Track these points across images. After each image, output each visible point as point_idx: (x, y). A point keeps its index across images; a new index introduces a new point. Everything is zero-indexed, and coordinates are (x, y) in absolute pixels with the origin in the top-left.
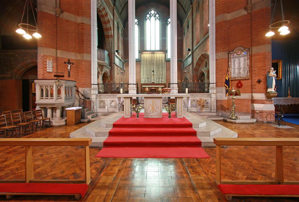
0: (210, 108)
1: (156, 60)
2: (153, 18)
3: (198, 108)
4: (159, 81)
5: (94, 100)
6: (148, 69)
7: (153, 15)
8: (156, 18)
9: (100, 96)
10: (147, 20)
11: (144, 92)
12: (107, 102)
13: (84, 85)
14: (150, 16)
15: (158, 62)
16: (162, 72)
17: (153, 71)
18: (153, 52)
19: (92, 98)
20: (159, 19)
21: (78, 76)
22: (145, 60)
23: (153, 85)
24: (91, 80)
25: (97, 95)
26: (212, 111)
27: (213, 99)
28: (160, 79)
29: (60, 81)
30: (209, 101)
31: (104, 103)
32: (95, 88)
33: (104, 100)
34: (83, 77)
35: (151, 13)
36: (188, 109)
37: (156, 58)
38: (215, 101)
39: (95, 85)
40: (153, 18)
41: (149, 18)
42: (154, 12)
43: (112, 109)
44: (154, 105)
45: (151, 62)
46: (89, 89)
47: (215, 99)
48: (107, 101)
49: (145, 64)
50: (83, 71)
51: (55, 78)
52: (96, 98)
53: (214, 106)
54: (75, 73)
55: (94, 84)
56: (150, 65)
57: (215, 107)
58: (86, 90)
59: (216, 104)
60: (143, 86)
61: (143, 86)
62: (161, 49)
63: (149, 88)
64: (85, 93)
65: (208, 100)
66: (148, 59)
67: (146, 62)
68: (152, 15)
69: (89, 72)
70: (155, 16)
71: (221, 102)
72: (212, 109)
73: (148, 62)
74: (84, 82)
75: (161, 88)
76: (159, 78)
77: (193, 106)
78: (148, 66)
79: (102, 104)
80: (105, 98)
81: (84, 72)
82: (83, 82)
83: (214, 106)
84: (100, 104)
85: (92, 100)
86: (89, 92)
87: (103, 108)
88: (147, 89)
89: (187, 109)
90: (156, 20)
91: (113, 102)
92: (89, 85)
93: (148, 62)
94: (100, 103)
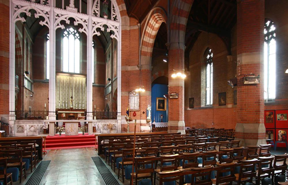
2: (71, 36)
4: (78, 107)
7: (72, 33)
8: (76, 37)
10: (64, 37)
14: (69, 34)
17: (72, 98)
18: (71, 74)
20: (80, 39)
22: (62, 81)
35: (69, 31)
40: (71, 36)
41: (67, 36)
42: (73, 30)
45: (69, 85)
49: (61, 87)
56: (68, 88)
60: (59, 112)
61: (59, 112)
62: (82, 73)
66: (65, 82)
68: (70, 33)
70: (74, 35)
73: (65, 85)
75: (80, 114)
78: (65, 89)
90: (76, 39)
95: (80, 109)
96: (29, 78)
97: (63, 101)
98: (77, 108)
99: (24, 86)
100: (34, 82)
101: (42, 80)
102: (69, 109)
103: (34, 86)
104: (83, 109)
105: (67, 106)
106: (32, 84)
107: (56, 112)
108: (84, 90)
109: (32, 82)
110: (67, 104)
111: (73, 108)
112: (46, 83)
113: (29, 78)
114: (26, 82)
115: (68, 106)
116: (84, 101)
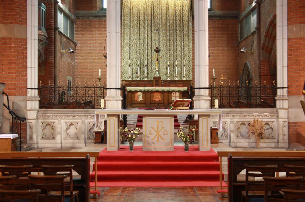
0: (276, 140)
1: (164, 13)
3: (251, 140)
4: (172, 75)
5: (34, 121)
6: (142, 38)
11: (132, 104)
13: (15, 89)
15: (171, 18)
16: (182, 50)
17: (158, 51)
21: (2, 70)
23: (157, 85)
25: (38, 111)
26: (280, 145)
27: (281, 121)
28: (177, 69)
30: (275, 125)
31: (53, 129)
33: (54, 123)
36: (230, 142)
37: (164, 9)
38: (286, 124)
43: (71, 141)
44: (160, 128)
47: (286, 120)
49: (134, 24)
52: (37, 118)
53: (284, 135)
56: (149, 28)
57: (286, 137)
59: (289, 131)
60: (129, 88)
61: (129, 88)
63: (144, 92)
65: (273, 122)
66: (141, 13)
67: (135, 19)
71: (295, 126)
72: (280, 141)
73: (142, 18)
74: (15, 84)
75: (178, 94)
76: (174, 66)
77: (242, 136)
79: (48, 130)
80: (56, 118)
82: (12, 84)
83: (284, 135)
84: (45, 131)
86: (22, 104)
87: (52, 139)
88: (140, 97)
89: (228, 141)
92: (23, 90)
93: (142, 18)
95: (177, 79)
96: (66, 10)
97: (138, 63)
98: (169, 79)
99: (56, 29)
100: (78, 17)
101: (93, 12)
102: (151, 81)
103: (78, 28)
104: (184, 79)
105: (146, 73)
106: (72, 23)
107: (123, 89)
108: (186, 28)
109: (73, 17)
110: (148, 69)
111: (159, 78)
112: (101, 17)
113: (66, 10)
114: (60, 18)
115: (148, 73)
116: (187, 58)
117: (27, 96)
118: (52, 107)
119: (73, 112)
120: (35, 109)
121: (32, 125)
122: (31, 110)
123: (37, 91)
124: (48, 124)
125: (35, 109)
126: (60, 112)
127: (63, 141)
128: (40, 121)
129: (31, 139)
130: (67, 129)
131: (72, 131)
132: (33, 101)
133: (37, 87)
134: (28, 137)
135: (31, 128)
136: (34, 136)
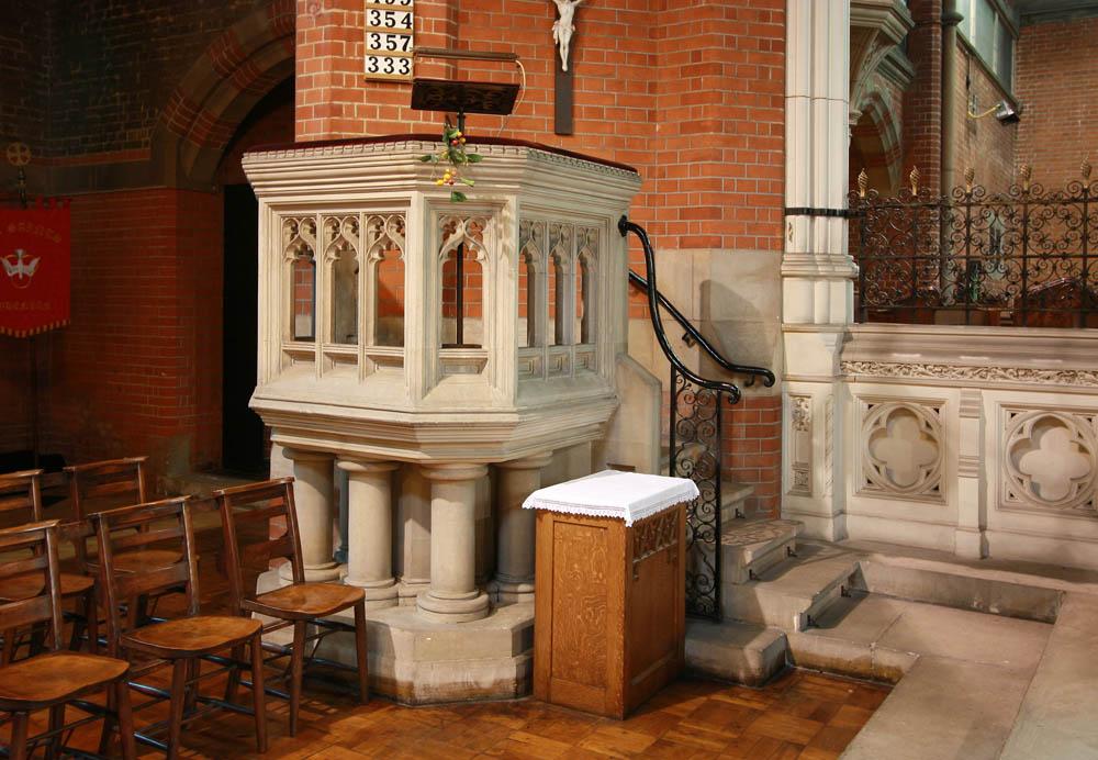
5: (819, 392)
9: (883, 349)
12: (969, 425)
13: (715, 213)
19: (790, 372)
21: (652, 116)
24: (783, 159)
25: (847, 338)
29: (470, 149)
31: (930, 438)
32: (828, 259)
34: (700, 127)
39: (820, 220)
43: (1048, 523)
46: (752, 260)
48: (972, 410)
50: (697, 56)
51: (433, 121)
52: (840, 375)
54: (619, 85)
55: (811, 212)
58: (732, 270)
64: (716, 314)
69: (764, 72)
74: (715, 184)
80: (947, 378)
81: (718, 69)
82: (698, 184)
84: (882, 445)
85: (796, 387)
86: (754, 295)
91: (1054, 433)
92: (762, 217)
94: (873, 437)
117: (783, 249)
118: (928, 319)
119: (1062, 350)
120: (827, 325)
121: (811, 408)
122: (808, 326)
123: (839, 227)
124: (903, 411)
125: (827, 325)
126: (975, 348)
127: (993, 517)
128: (856, 388)
129: (805, 486)
130: (1019, 448)
131: (1053, 458)
132: (815, 277)
133: (839, 204)
134: (789, 477)
135: (803, 425)
136: (823, 476)
